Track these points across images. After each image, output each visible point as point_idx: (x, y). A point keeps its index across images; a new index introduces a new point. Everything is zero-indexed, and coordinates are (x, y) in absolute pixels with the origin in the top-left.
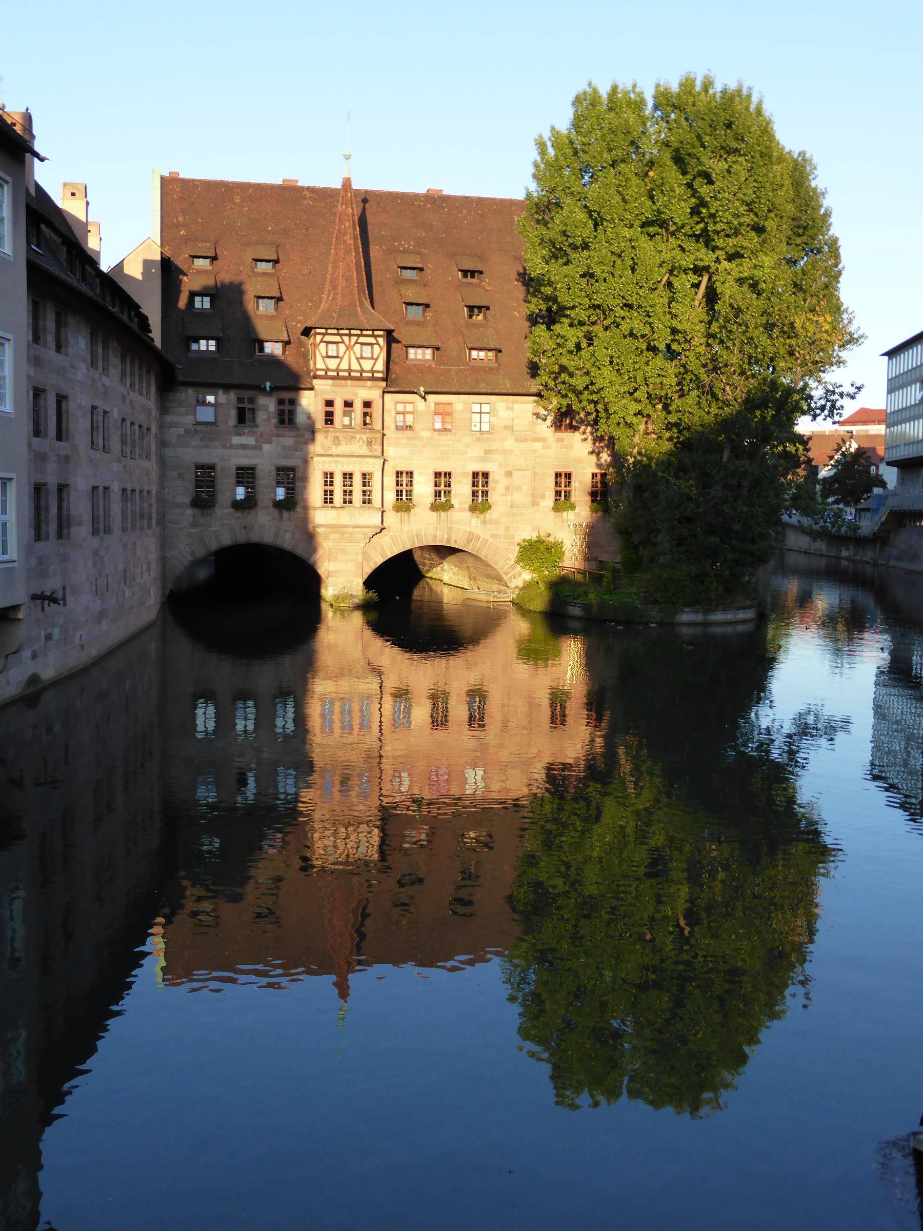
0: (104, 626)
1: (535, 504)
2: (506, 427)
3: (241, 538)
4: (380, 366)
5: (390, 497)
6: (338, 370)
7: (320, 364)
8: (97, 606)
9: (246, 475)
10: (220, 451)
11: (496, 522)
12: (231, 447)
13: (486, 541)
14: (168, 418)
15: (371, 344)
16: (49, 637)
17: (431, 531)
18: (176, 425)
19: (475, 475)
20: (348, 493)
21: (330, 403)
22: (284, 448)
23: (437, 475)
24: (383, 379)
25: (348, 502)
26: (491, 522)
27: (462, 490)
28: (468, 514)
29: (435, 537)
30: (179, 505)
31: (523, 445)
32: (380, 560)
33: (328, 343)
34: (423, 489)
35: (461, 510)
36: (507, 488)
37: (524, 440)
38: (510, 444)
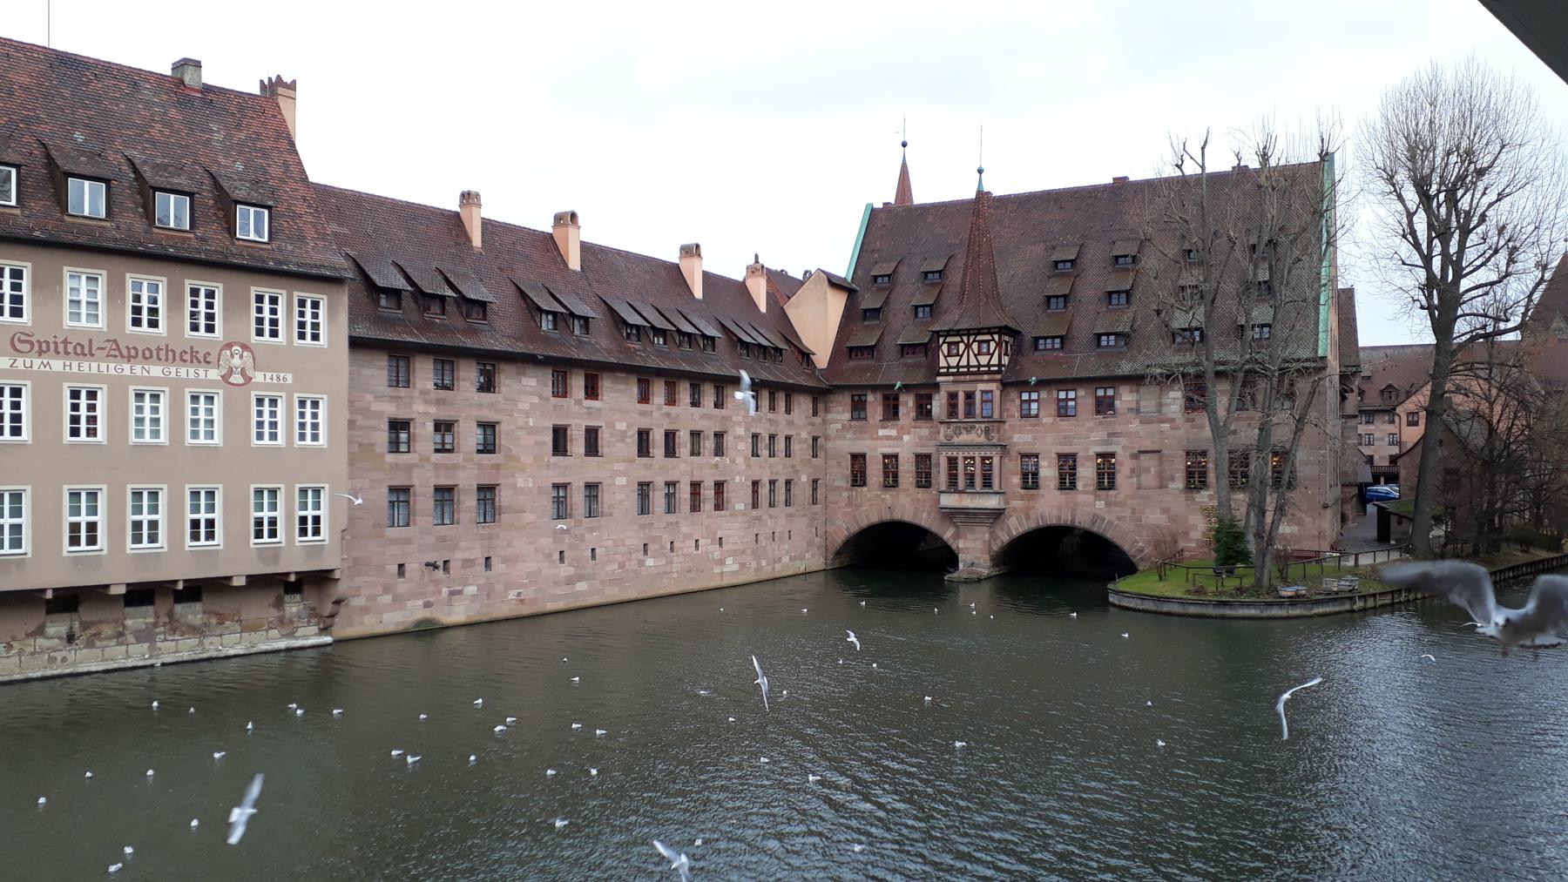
0: (582, 586)
1: (1162, 486)
2: (1130, 410)
3: (887, 517)
4: (995, 361)
5: (1016, 480)
6: (958, 366)
7: (943, 363)
8: (565, 570)
9: (891, 461)
10: (869, 442)
11: (1122, 505)
12: (879, 438)
13: (1110, 523)
14: (830, 416)
15: (988, 342)
16: (452, 593)
17: (1055, 512)
18: (836, 421)
19: (1099, 455)
20: (971, 478)
21: (953, 396)
22: (921, 438)
23: (1060, 456)
24: (999, 372)
25: (972, 484)
26: (1116, 504)
27: (1086, 473)
28: (1091, 497)
29: (1059, 518)
30: (838, 488)
31: (1149, 427)
32: (1006, 539)
33: (950, 344)
34: (1048, 472)
35: (1088, 493)
36: (1132, 471)
37: (1150, 422)
38: (1135, 426)
